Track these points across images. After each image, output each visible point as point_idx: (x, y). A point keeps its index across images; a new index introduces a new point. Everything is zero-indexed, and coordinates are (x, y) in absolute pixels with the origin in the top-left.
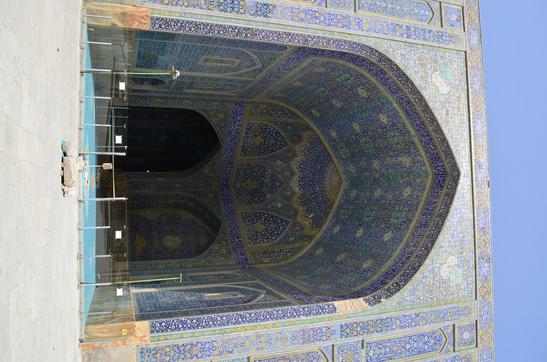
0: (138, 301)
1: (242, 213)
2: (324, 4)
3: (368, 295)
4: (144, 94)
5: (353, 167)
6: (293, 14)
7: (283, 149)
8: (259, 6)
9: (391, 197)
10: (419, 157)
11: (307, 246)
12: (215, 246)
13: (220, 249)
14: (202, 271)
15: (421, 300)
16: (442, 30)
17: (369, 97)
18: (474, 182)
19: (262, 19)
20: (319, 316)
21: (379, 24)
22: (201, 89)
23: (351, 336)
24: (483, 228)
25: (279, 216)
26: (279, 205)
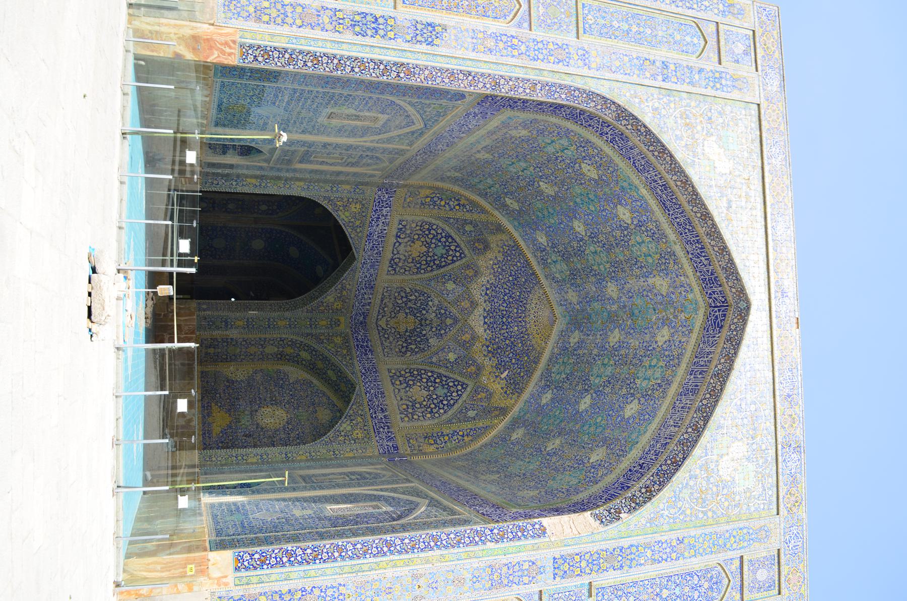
0: (214, 517)
1: (389, 371)
2: (526, 25)
3: (598, 506)
4: (227, 171)
5: (574, 294)
6: (474, 41)
7: (457, 263)
8: (419, 27)
9: (637, 343)
10: (682, 278)
11: (497, 425)
12: (344, 426)
13: (353, 430)
14: (322, 467)
15: (686, 516)
17: (600, 178)
19: (424, 48)
20: (518, 543)
21: (617, 59)
22: (322, 163)
23: (571, 577)
24: (789, 396)
26: (452, 357)
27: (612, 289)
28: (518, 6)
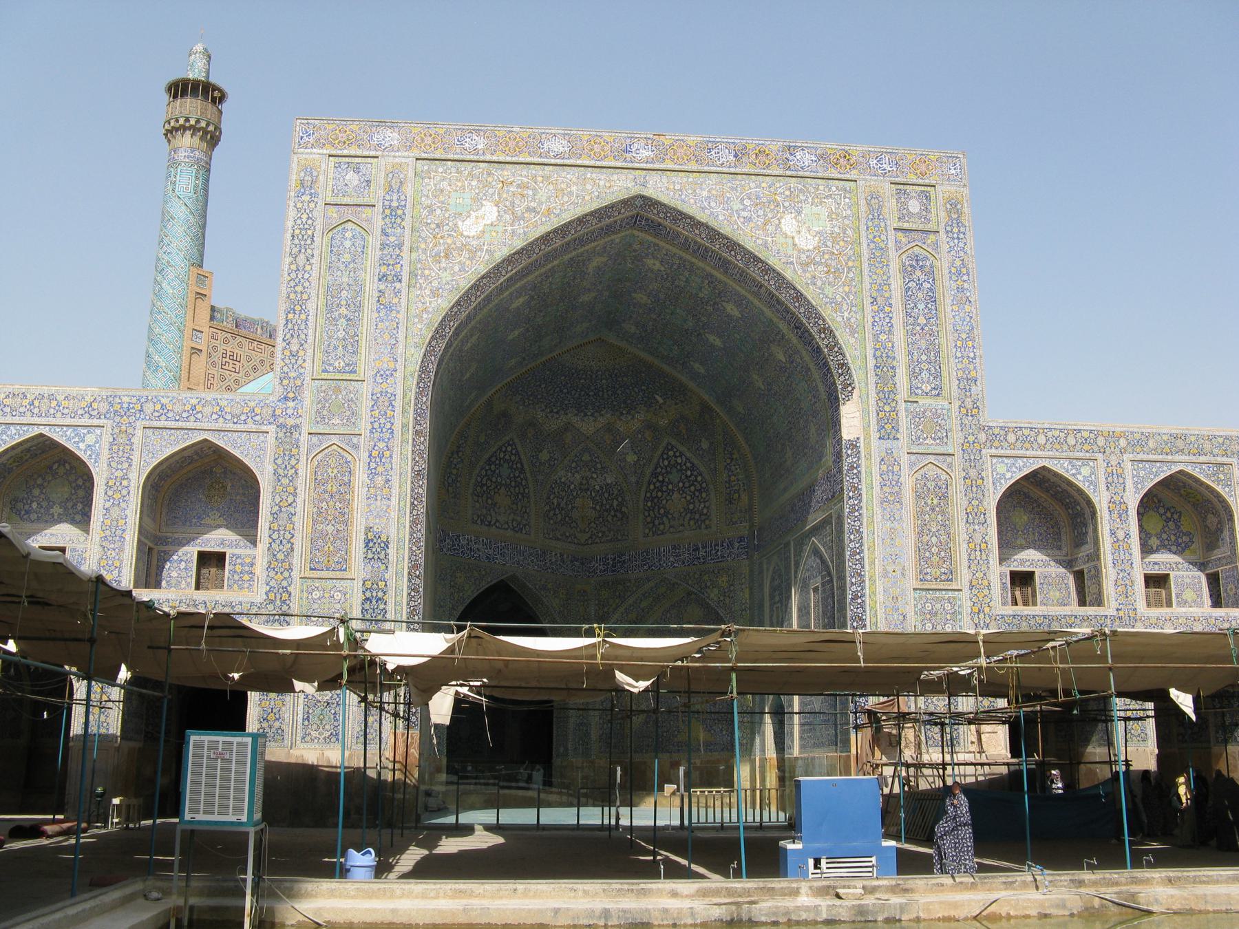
0: (815, 746)
1: (646, 536)
2: (355, 440)
7: (519, 448)
8: (370, 555)
16: (379, 208)
18: (656, 166)
19: (391, 551)
20: (864, 475)
23: (897, 422)
24: (736, 156)
25: (655, 461)
27: (586, 298)
28: (334, 447)
